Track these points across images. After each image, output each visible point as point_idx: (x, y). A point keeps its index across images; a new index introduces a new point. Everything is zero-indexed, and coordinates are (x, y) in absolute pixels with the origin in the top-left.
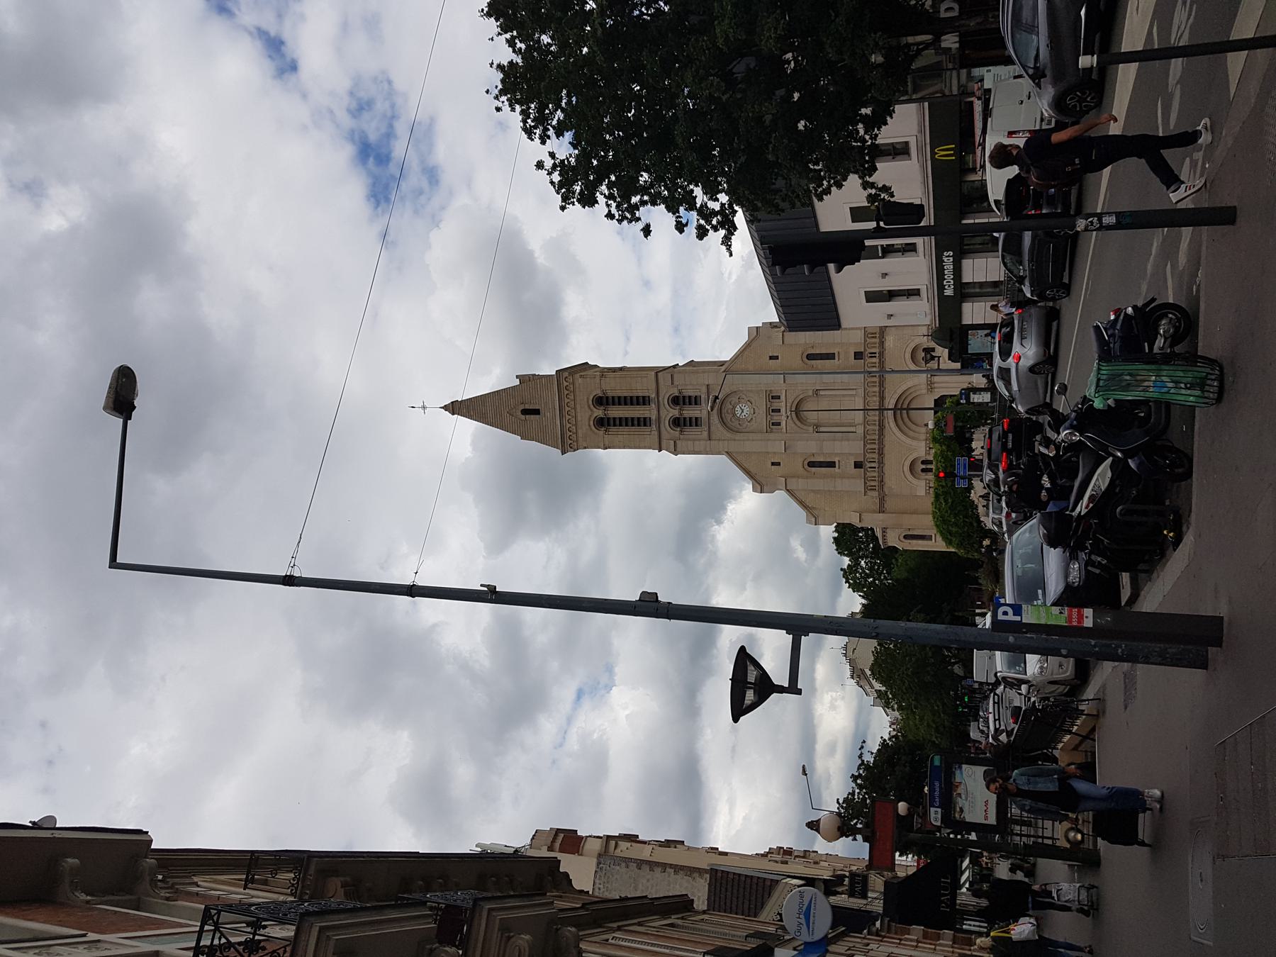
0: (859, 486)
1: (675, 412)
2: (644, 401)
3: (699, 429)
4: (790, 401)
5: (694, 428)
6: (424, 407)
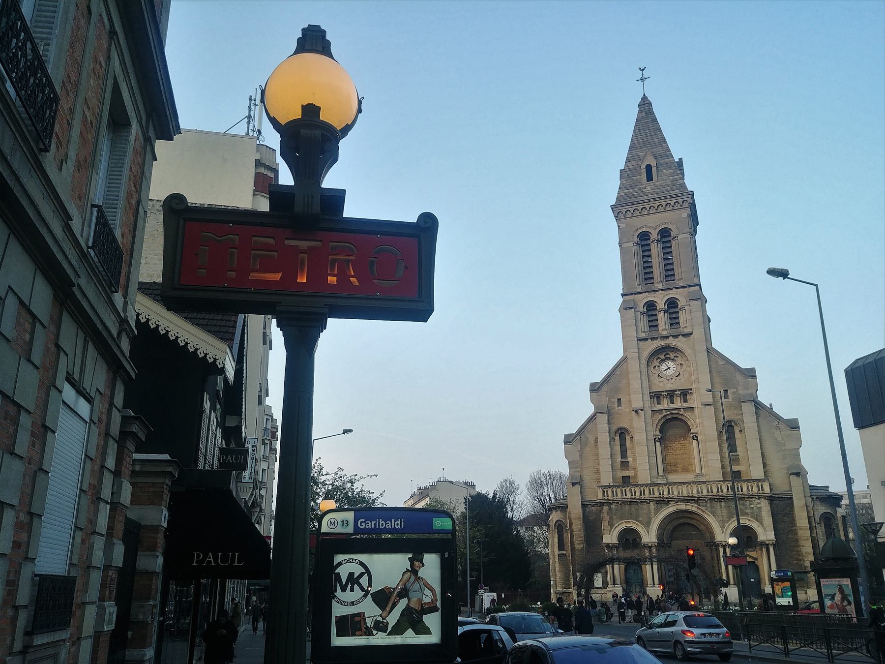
1: (661, 305)
2: (669, 274)
3: (647, 329)
5: (646, 324)
6: (643, 79)
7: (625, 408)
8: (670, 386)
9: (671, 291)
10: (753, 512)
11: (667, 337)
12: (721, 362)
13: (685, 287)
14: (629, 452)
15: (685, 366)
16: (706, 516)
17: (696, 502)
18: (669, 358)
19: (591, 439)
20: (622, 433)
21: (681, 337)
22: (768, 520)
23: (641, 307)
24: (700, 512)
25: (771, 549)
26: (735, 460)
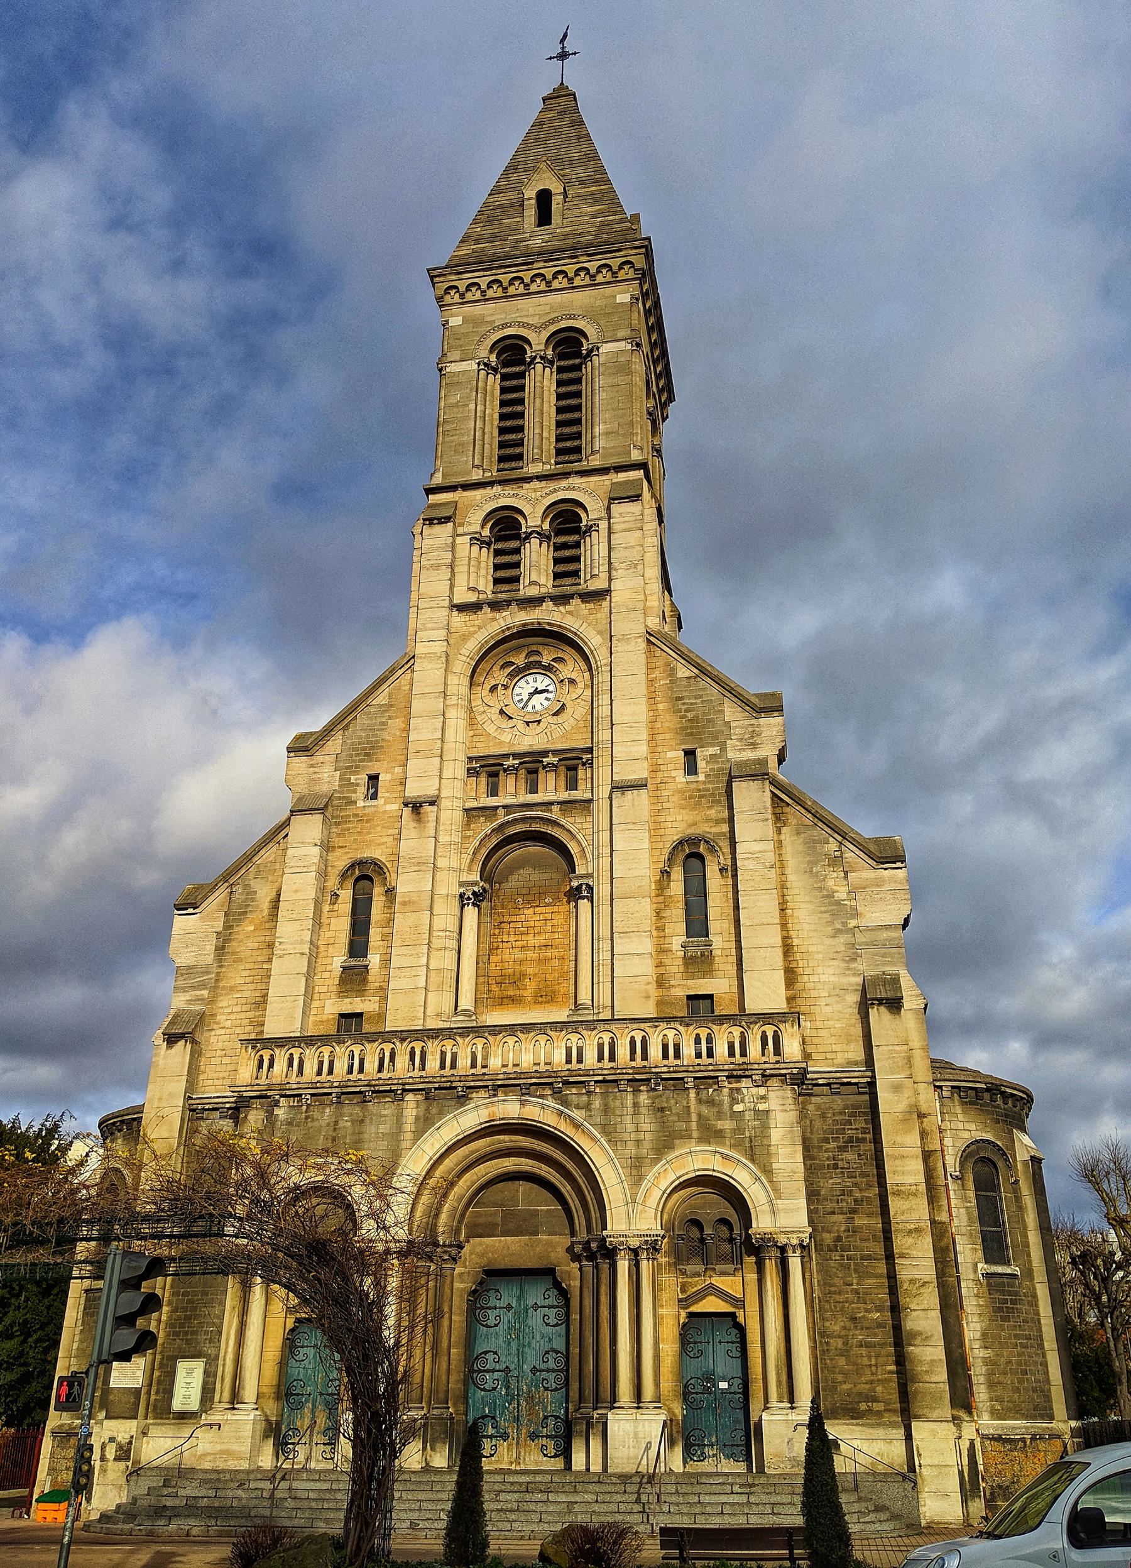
1: (534, 517)
2: (570, 445)
7: (388, 804)
8: (530, 740)
9: (564, 483)
10: (739, 1130)
11: (538, 601)
12: (683, 671)
13: (604, 471)
14: (375, 936)
15: (581, 685)
16: (582, 1142)
17: (557, 1093)
18: (538, 665)
19: (264, 894)
20: (365, 876)
21: (576, 601)
22: (788, 1159)
23: (474, 522)
24: (565, 1129)
25: (795, 1263)
26: (699, 961)
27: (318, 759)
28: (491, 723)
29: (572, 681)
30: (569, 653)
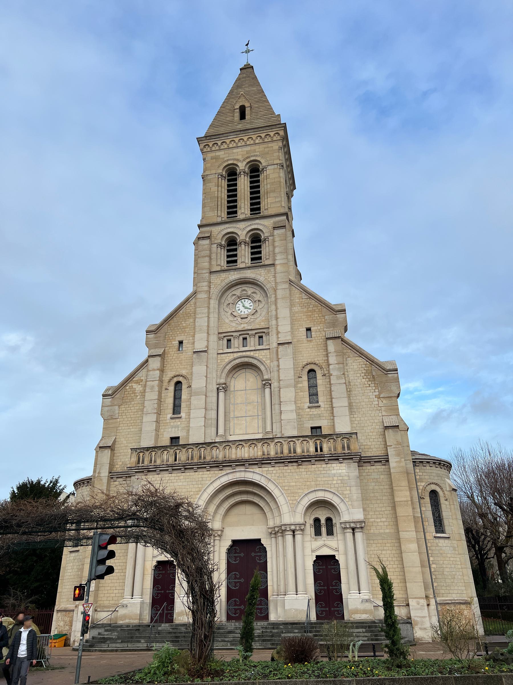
0: (147, 442)
4: (256, 354)
15: (264, 303)
27: (158, 335)
28: (227, 319)
29: (259, 301)
30: (258, 290)
